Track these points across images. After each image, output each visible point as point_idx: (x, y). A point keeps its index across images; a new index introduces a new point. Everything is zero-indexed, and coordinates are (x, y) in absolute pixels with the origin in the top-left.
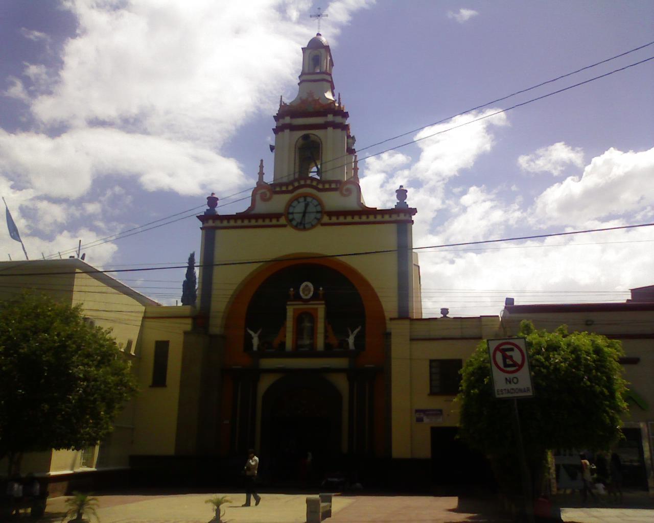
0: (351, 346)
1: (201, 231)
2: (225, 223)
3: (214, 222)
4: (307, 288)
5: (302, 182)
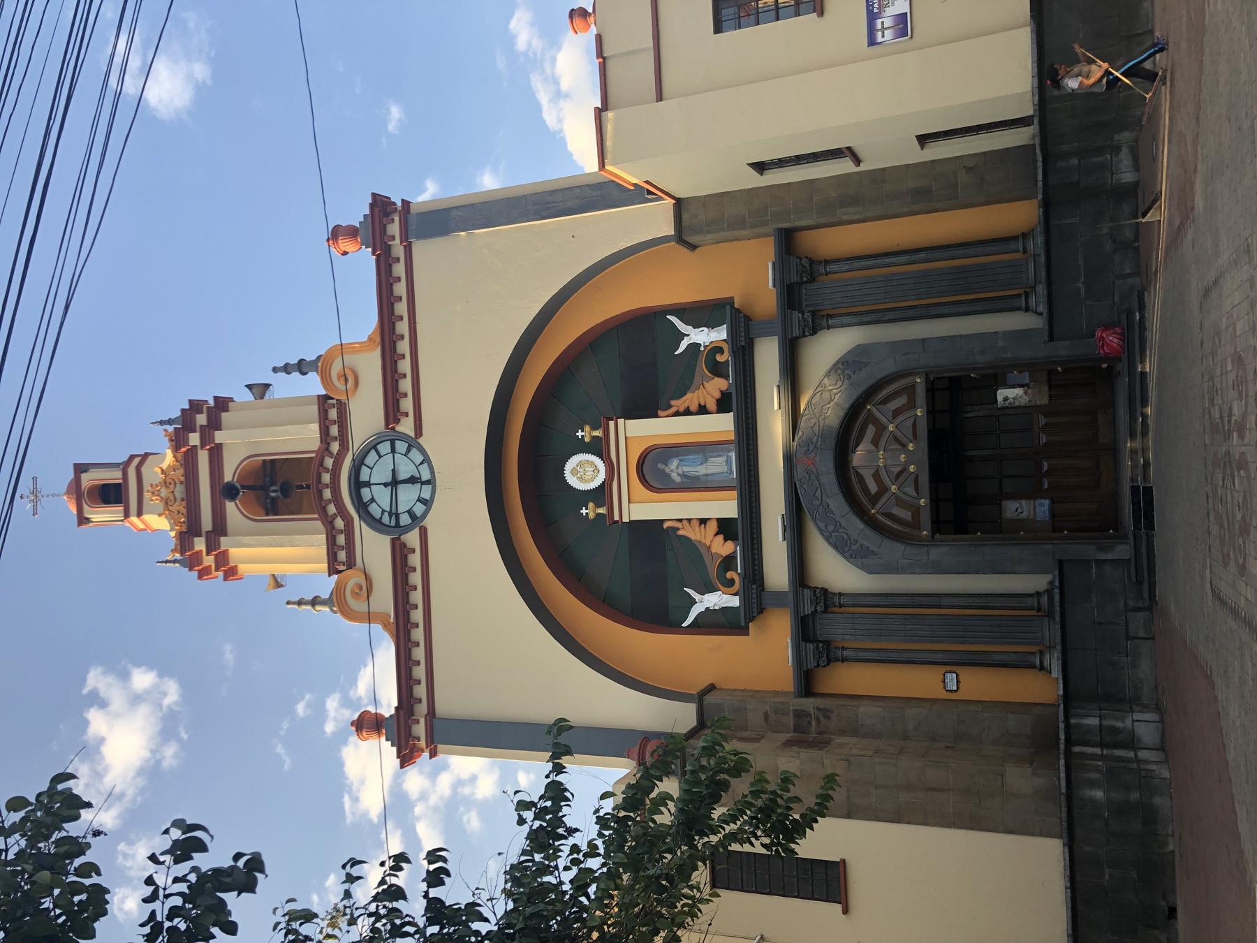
0: (719, 335)
1: (440, 757)
2: (420, 691)
3: (418, 722)
4: (583, 472)
5: (327, 494)
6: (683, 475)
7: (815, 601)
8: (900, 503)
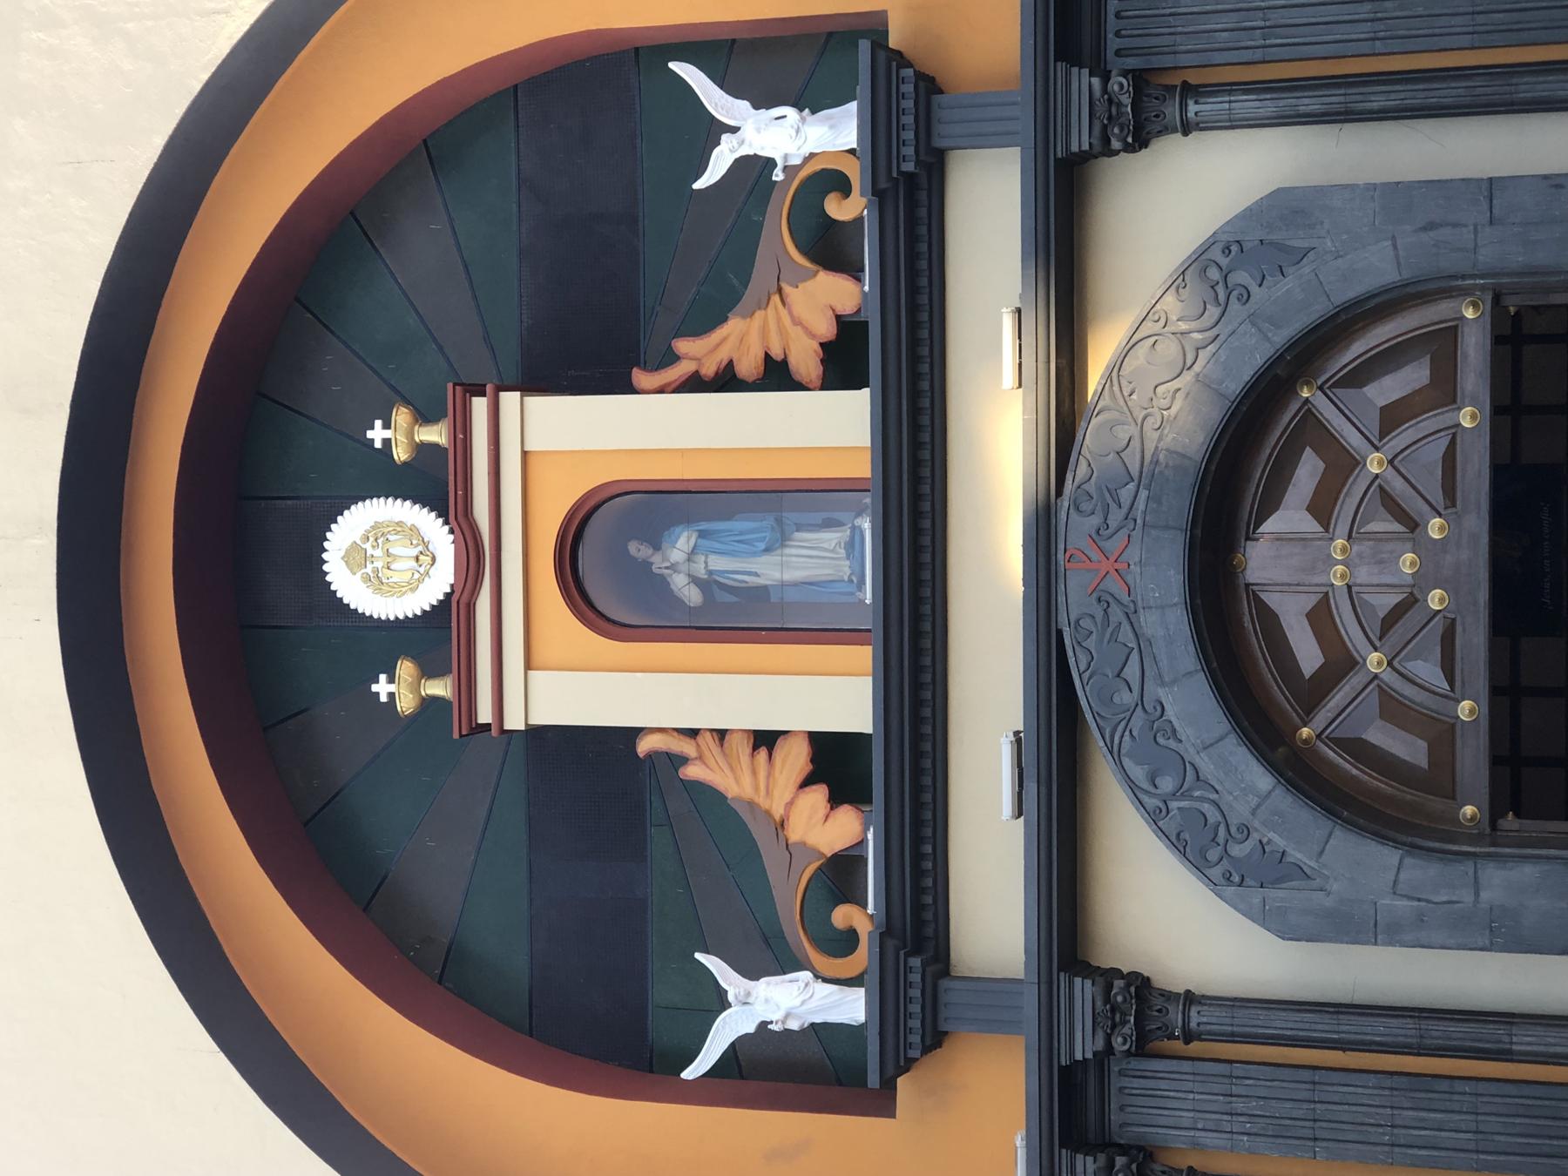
4: (382, 559)
6: (707, 585)
7: (1109, 1017)
8: (1393, 709)
